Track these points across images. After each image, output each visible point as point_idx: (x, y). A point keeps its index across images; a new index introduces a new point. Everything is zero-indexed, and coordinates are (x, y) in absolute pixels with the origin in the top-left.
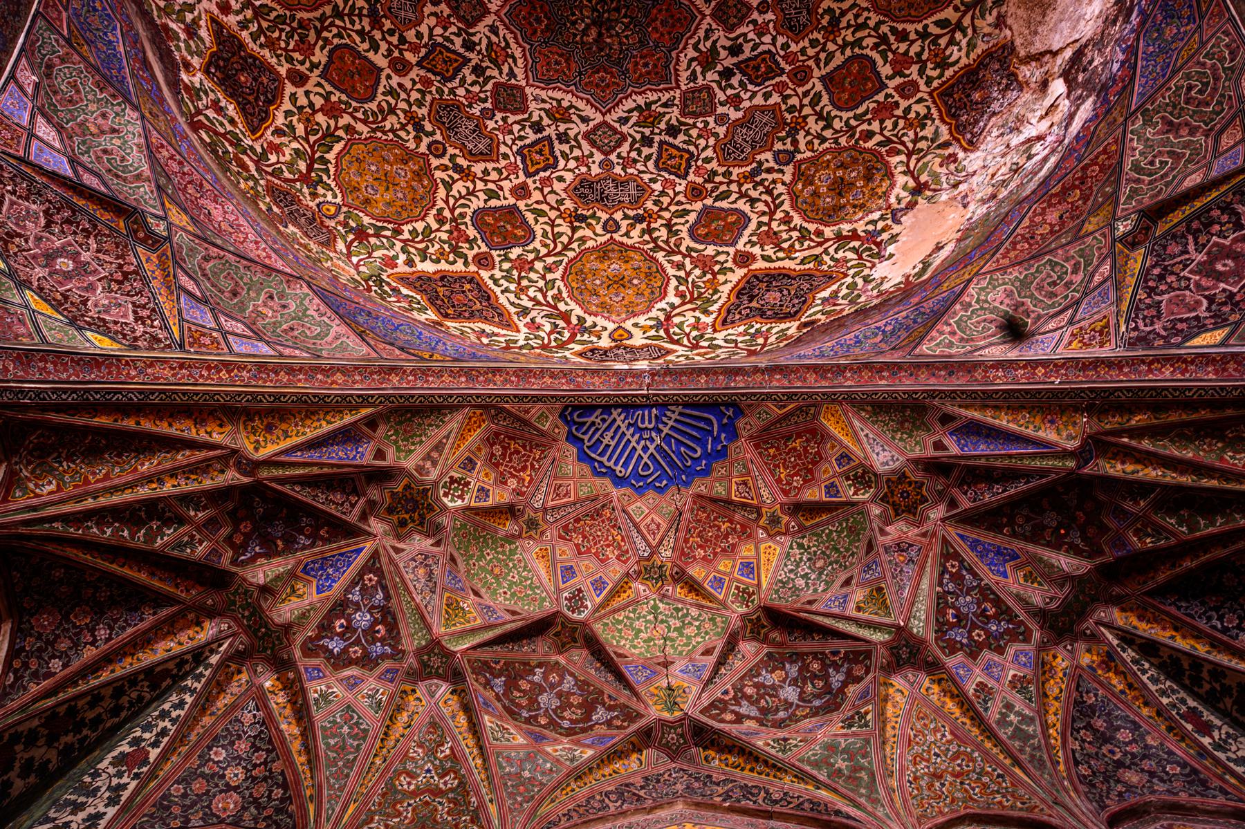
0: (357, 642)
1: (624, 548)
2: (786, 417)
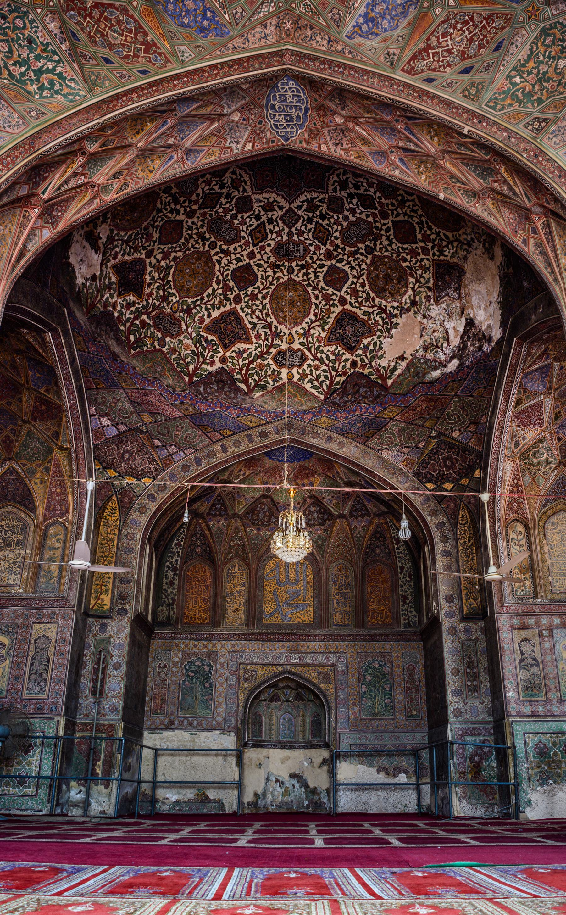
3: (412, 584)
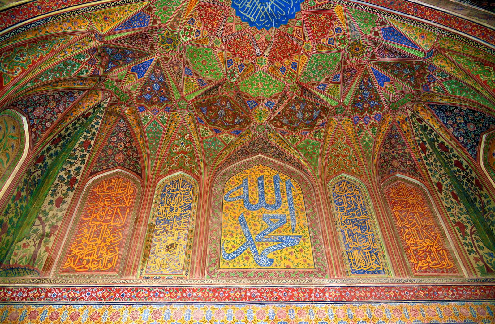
0: (155, 95)
1: (251, 52)
2: (321, 5)
3: (462, 206)
